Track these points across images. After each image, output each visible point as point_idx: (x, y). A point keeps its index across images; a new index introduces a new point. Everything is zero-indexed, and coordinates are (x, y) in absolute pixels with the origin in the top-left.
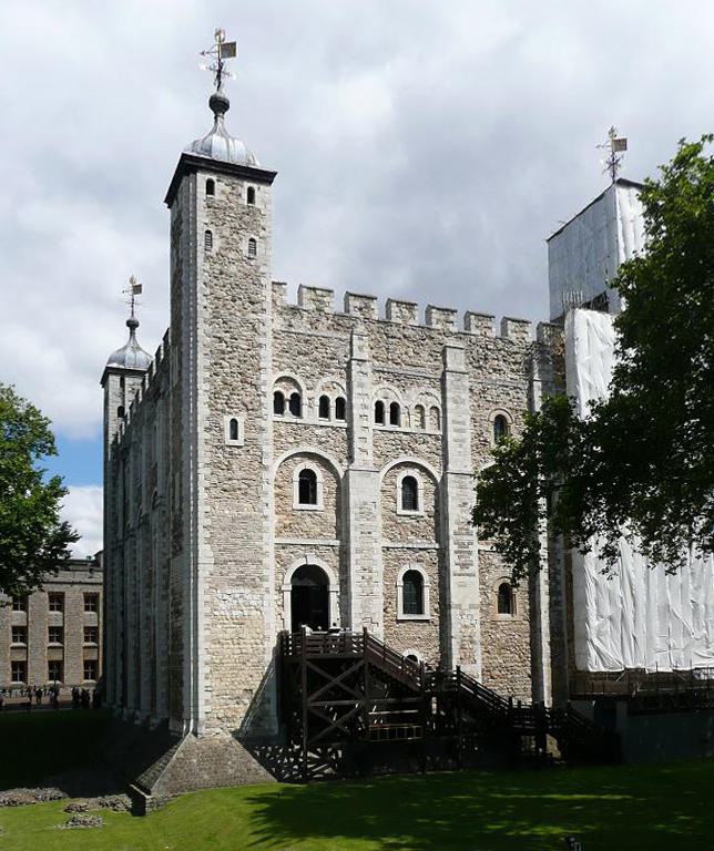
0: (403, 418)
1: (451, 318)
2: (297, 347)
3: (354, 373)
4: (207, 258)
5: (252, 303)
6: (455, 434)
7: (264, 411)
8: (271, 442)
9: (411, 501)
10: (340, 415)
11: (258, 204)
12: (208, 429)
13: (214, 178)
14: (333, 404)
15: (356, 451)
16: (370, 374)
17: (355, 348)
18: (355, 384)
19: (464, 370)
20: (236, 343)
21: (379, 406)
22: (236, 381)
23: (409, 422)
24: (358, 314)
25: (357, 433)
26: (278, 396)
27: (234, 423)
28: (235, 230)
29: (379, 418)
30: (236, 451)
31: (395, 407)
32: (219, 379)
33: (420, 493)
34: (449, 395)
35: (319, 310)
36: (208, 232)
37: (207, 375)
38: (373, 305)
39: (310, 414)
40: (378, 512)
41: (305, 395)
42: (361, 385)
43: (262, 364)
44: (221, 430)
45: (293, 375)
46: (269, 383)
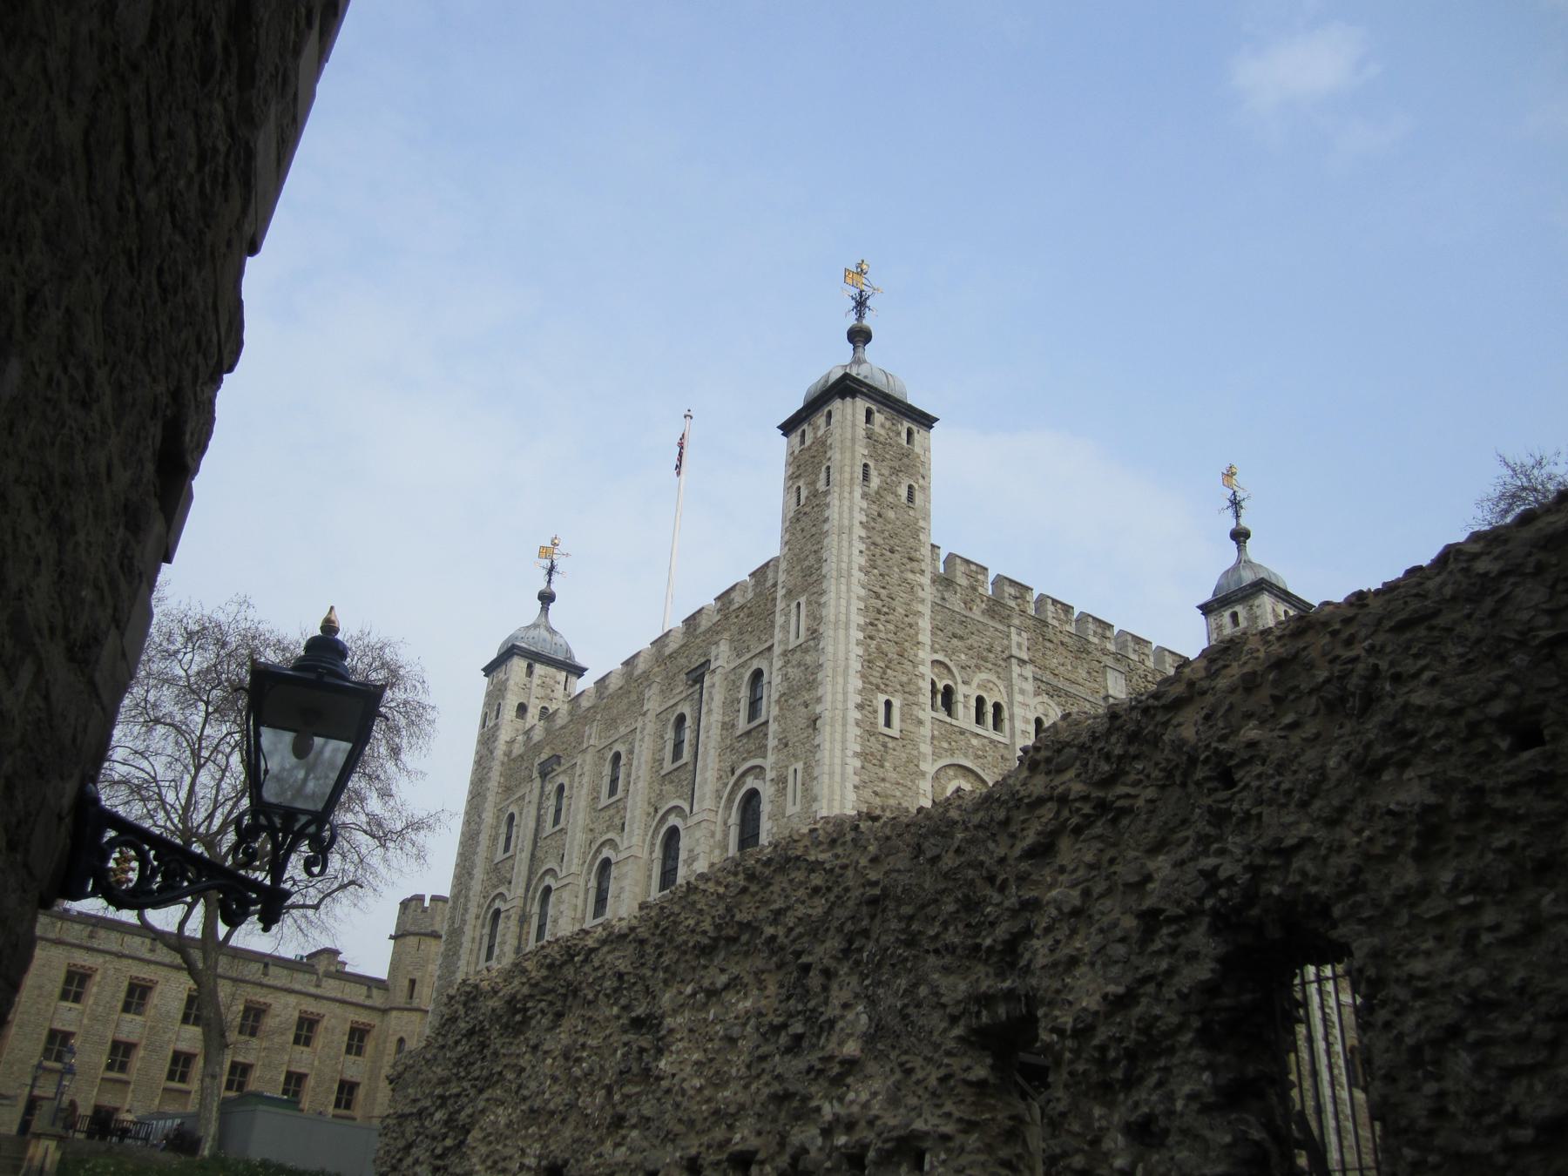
2: (951, 629)
3: (1015, 675)
4: (865, 496)
5: (911, 559)
7: (922, 699)
8: (928, 740)
10: (997, 725)
12: (860, 707)
13: (874, 408)
14: (989, 710)
18: (1016, 688)
20: (894, 604)
22: (892, 651)
24: (1013, 604)
27: (888, 704)
30: (891, 744)
32: (873, 644)
35: (974, 589)
36: (866, 466)
37: (861, 636)
41: (961, 691)
42: (1022, 692)
43: (921, 638)
44: (876, 712)
45: (947, 661)
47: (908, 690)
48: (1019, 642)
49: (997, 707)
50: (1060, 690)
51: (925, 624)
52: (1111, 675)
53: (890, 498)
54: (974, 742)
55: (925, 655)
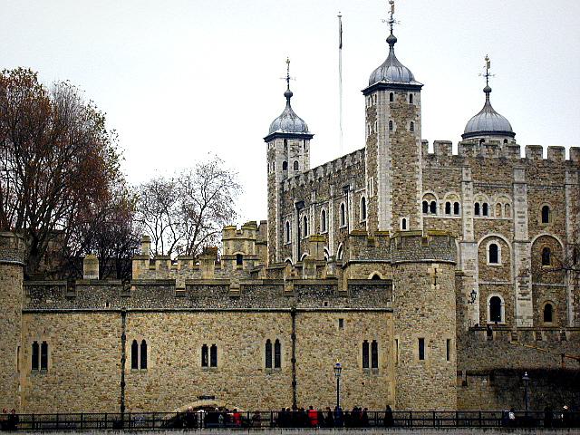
0: (489, 212)
1: (517, 151)
3: (463, 189)
6: (519, 219)
7: (418, 214)
9: (494, 258)
10: (456, 212)
11: (414, 104)
12: (392, 225)
14: (452, 206)
15: (465, 231)
16: (472, 187)
17: (464, 175)
19: (523, 180)
21: (477, 205)
23: (493, 214)
25: (465, 222)
26: (425, 203)
27: (404, 220)
28: (404, 119)
29: (477, 212)
31: (485, 205)
33: (499, 253)
34: (515, 197)
38: (474, 149)
39: (441, 213)
40: (476, 265)
41: (438, 202)
42: (467, 195)
45: (432, 192)
46: (420, 197)
47: (413, 212)
48: (467, 175)
49: (456, 205)
50: (488, 187)
51: (419, 183)
52: (516, 172)
53: (402, 133)
54: (445, 222)
55: (420, 195)
